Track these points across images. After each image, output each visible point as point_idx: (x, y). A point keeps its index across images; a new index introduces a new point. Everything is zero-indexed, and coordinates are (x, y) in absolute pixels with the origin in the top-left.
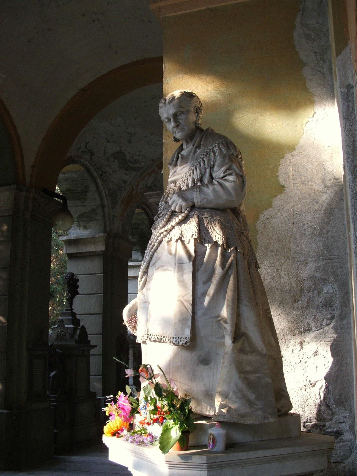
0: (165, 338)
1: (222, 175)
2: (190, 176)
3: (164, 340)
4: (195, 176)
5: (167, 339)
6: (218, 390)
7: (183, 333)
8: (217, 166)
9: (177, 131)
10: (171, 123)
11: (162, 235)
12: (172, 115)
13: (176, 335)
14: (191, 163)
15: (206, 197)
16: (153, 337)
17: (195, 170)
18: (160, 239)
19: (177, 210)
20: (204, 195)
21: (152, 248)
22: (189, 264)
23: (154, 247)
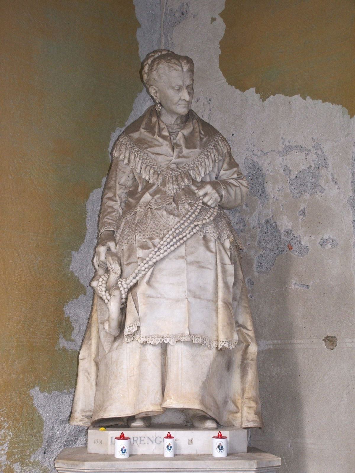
0: (207, 341)
1: (235, 176)
2: (201, 164)
3: (205, 343)
4: (208, 167)
5: (208, 343)
6: (248, 396)
7: (232, 338)
8: (227, 164)
9: (184, 105)
10: (178, 93)
11: (197, 228)
12: (187, 85)
13: (227, 339)
14: (201, 150)
15: (230, 197)
16: (196, 339)
17: (207, 161)
18: (194, 231)
19: (209, 203)
20: (229, 194)
21: (182, 238)
22: (230, 266)
23: (185, 239)
